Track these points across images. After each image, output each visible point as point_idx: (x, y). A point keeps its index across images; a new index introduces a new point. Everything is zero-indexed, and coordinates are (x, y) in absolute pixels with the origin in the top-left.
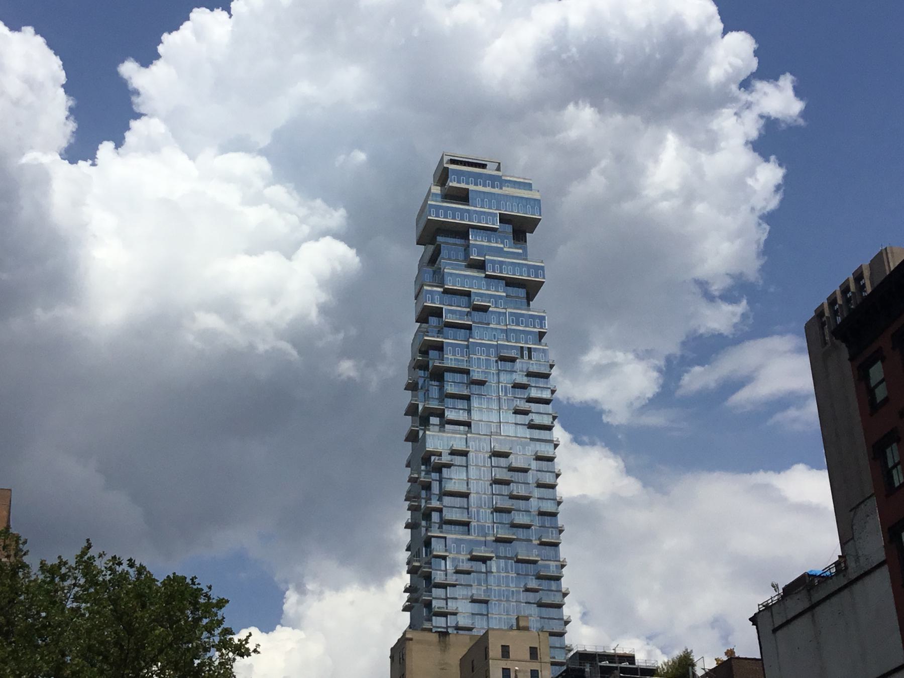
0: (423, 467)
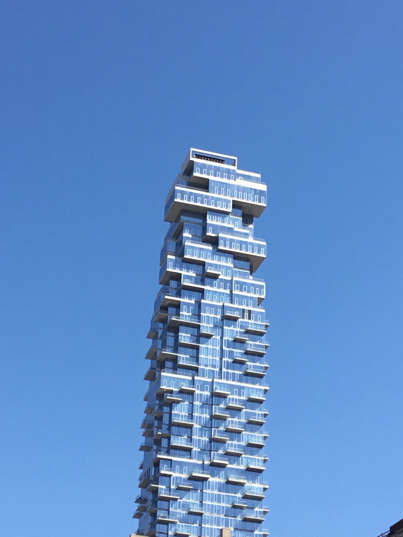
0: (158, 402)
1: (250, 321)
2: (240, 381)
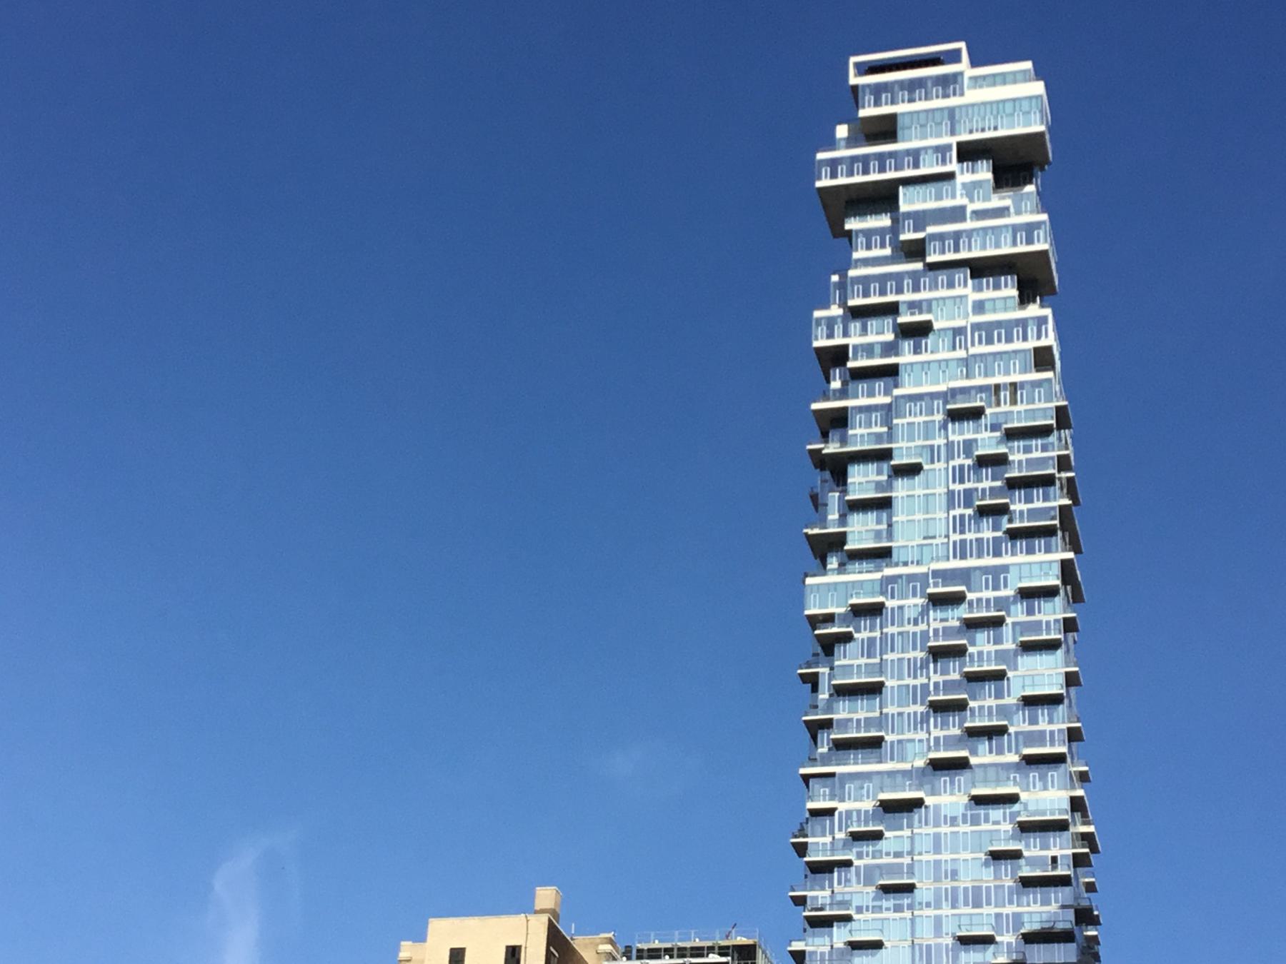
1: (1015, 409)
2: (997, 553)
